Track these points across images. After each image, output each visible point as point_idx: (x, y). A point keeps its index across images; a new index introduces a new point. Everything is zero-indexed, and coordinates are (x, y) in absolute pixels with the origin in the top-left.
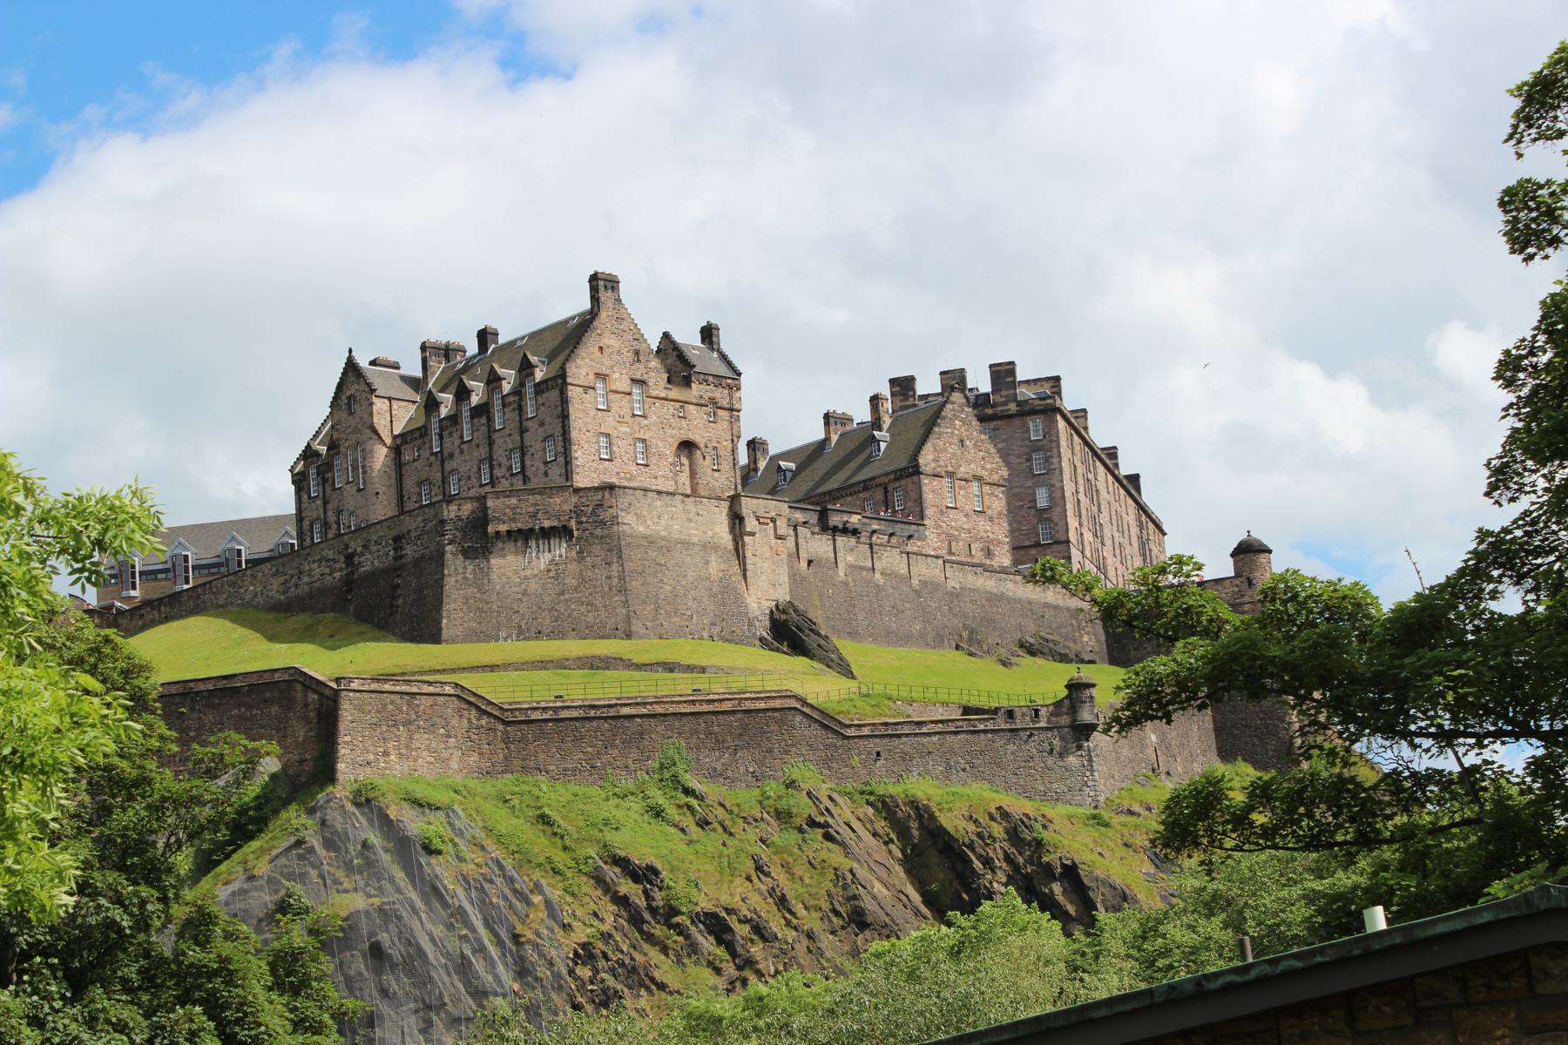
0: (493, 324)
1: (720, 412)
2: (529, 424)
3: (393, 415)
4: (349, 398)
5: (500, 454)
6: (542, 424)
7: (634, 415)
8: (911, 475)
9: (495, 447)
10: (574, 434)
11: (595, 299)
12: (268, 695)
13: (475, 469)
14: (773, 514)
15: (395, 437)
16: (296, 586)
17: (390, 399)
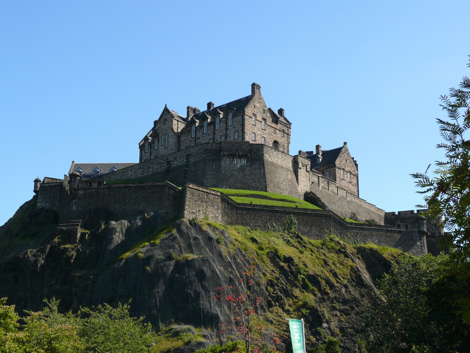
0: (213, 102)
1: (285, 135)
2: (229, 127)
3: (178, 127)
4: (164, 120)
5: (217, 137)
6: (234, 127)
8: (332, 167)
9: (216, 135)
10: (246, 130)
12: (155, 190)
14: (306, 164)
16: (147, 172)
17: (178, 121)
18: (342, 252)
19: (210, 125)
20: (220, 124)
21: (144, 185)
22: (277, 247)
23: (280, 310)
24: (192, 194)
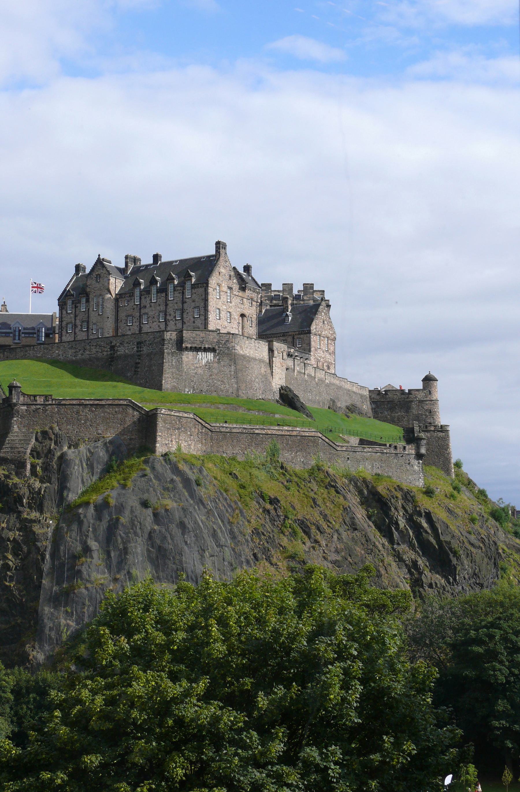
1: (254, 303)
4: (97, 275)
5: (170, 310)
6: (194, 301)
7: (227, 302)
8: (306, 333)
9: (168, 307)
13: (157, 314)
15: (116, 294)
18: (333, 486)
20: (174, 294)
22: (261, 484)
23: (267, 564)
24: (164, 421)
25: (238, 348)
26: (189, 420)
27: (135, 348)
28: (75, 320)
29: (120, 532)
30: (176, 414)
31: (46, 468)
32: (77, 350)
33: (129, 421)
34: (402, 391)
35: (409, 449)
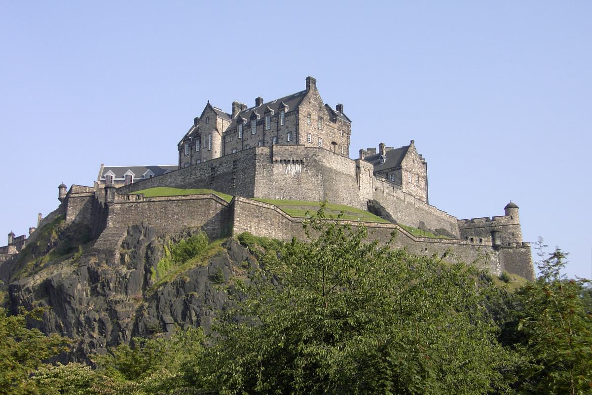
1: (345, 134)
2: (282, 127)
6: (287, 128)
8: (398, 169)
9: (266, 136)
10: (300, 132)
11: (308, 86)
15: (223, 133)
16: (189, 179)
19: (260, 125)
20: (271, 124)
21: (189, 198)
24: (243, 208)
25: (324, 160)
26: (269, 211)
27: (232, 166)
28: (191, 159)
29: (194, 306)
30: (255, 204)
31: (133, 256)
32: (186, 176)
33: (212, 214)
34: (487, 219)
35: (485, 241)
